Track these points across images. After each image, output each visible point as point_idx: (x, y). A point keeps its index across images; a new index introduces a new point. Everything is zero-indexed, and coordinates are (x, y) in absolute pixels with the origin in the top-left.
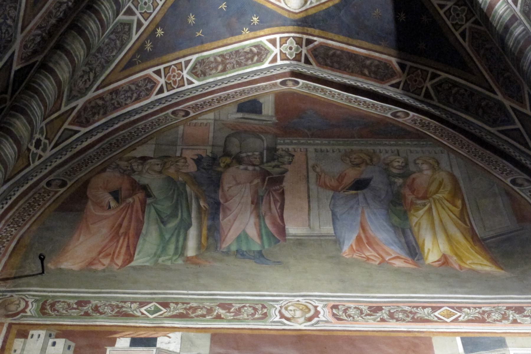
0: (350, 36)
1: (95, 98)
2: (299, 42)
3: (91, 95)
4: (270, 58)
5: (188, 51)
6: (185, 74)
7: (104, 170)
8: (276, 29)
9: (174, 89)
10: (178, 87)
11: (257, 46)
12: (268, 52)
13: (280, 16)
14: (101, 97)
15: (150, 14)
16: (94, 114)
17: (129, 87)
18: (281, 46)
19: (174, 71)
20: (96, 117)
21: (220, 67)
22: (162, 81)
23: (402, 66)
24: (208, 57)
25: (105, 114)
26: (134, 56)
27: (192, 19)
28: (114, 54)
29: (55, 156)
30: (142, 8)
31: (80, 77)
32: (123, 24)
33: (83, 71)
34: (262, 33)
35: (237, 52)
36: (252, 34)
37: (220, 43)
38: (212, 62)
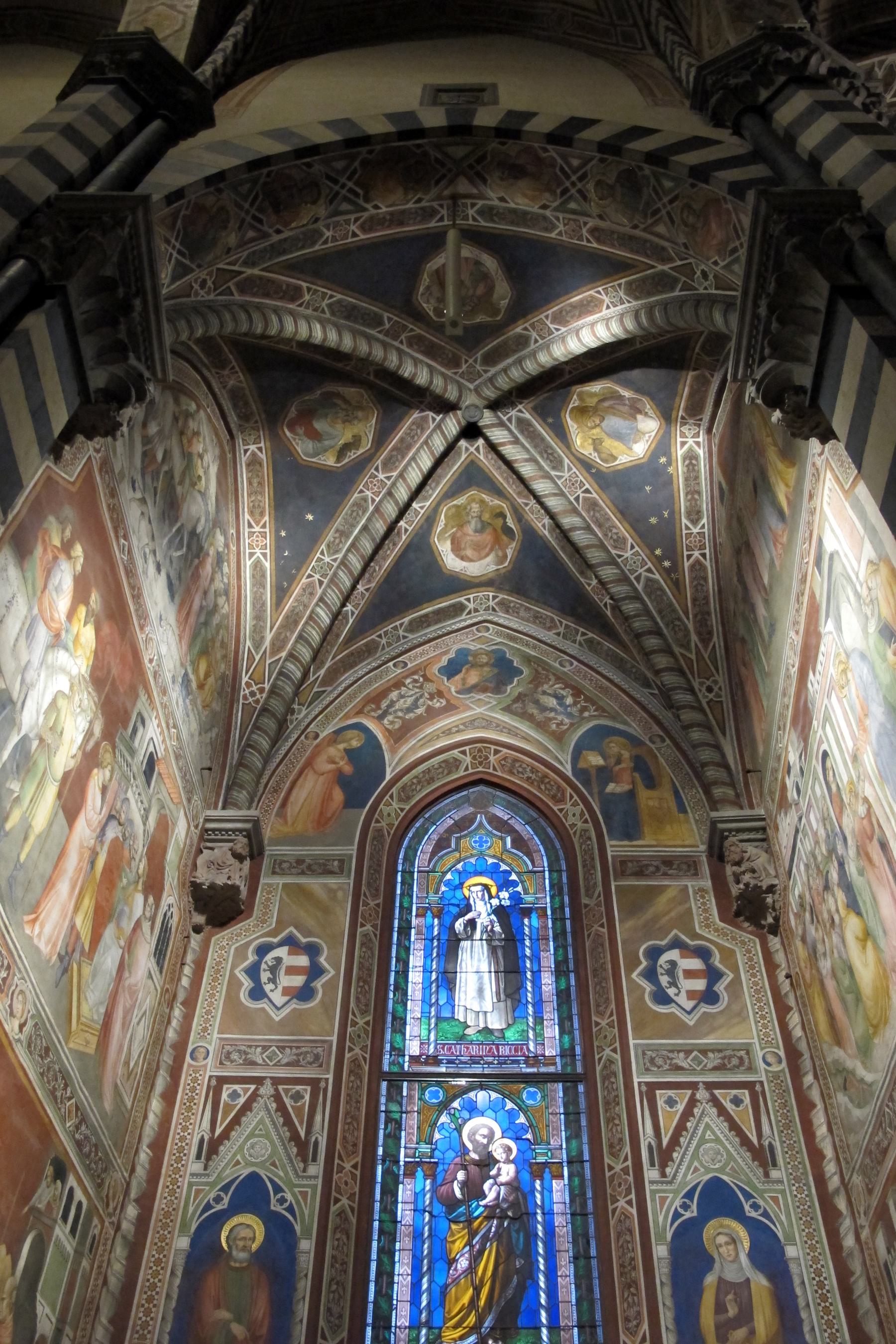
0: (676, 395)
1: (694, 622)
2: (683, 424)
3: (691, 626)
4: (696, 447)
5: (678, 526)
6: (695, 530)
8: (673, 441)
12: (690, 450)
13: (663, 437)
14: (695, 616)
16: (707, 625)
21: (696, 496)
22: (696, 554)
23: (695, 369)
24: (686, 507)
25: (709, 614)
26: (672, 579)
27: (653, 520)
32: (646, 586)
34: (674, 454)
35: (686, 479)
36: (674, 464)
37: (676, 494)
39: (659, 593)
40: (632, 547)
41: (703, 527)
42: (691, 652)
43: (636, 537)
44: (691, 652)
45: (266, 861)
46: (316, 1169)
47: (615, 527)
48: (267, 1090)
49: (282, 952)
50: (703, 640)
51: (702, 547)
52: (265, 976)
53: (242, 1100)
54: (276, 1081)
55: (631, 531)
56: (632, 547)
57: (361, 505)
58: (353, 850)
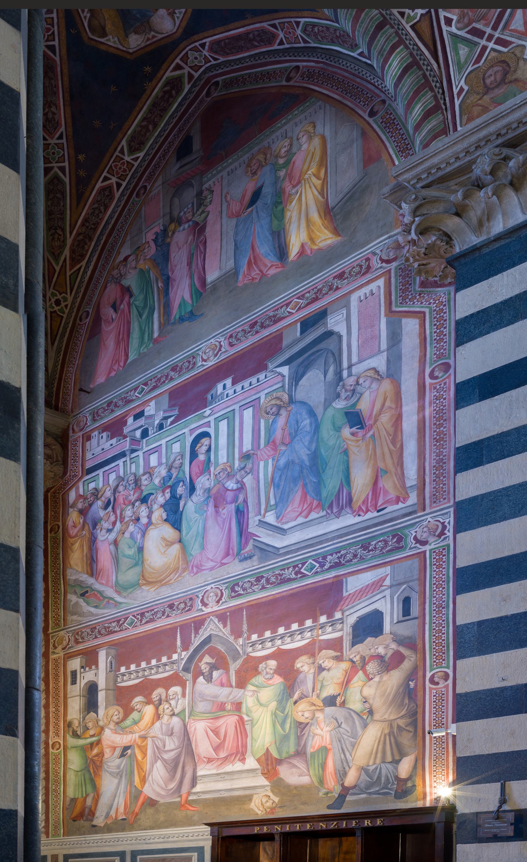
1: (74, 240)
3: (69, 242)
6: (127, 158)
7: (106, 287)
9: (128, 175)
10: (130, 171)
11: (167, 83)
14: (78, 234)
15: (64, 155)
16: (83, 247)
17: (93, 209)
18: (186, 64)
19: (116, 166)
20: (86, 247)
28: (62, 204)
29: (75, 298)
30: (54, 159)
31: (52, 240)
33: (51, 235)
38: (141, 131)
39: (59, 195)
40: (60, 137)
41: (136, 159)
42: (58, 264)
43: (70, 129)
44: (58, 264)
47: (57, 107)
50: (72, 259)
51: (122, 178)
55: (69, 120)
56: (60, 137)
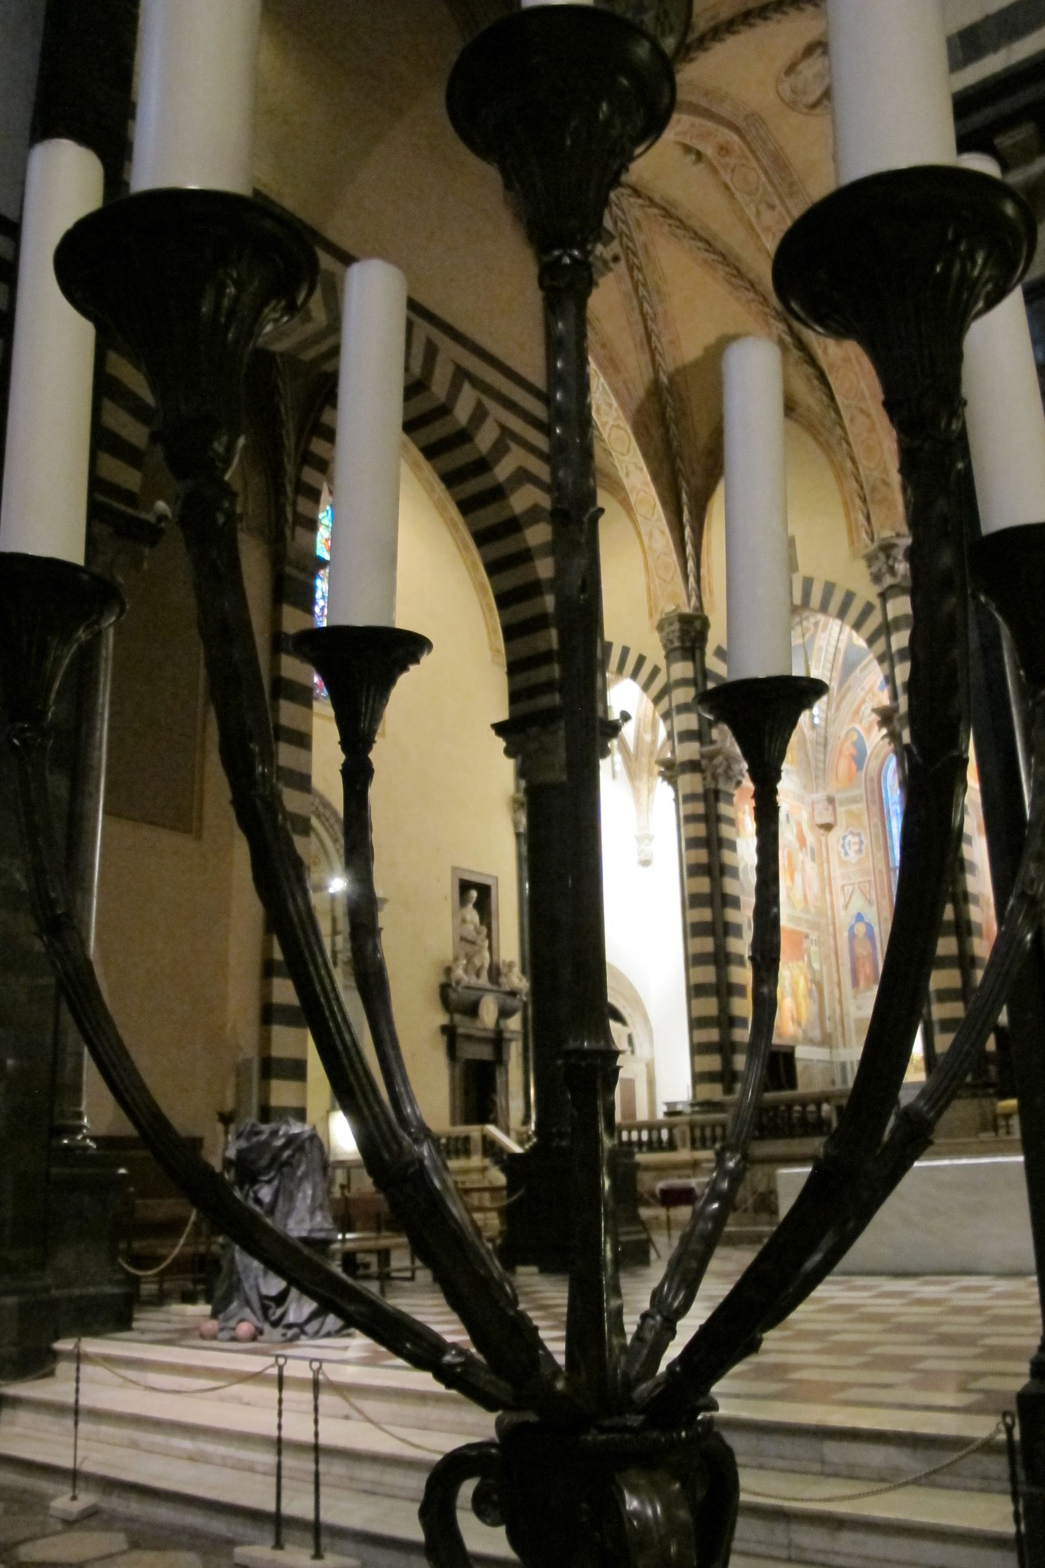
45: (837, 804)
46: (875, 907)
48: (856, 886)
49: (850, 838)
52: (847, 847)
53: (850, 891)
54: (858, 883)
57: (820, 648)
58: (863, 790)
